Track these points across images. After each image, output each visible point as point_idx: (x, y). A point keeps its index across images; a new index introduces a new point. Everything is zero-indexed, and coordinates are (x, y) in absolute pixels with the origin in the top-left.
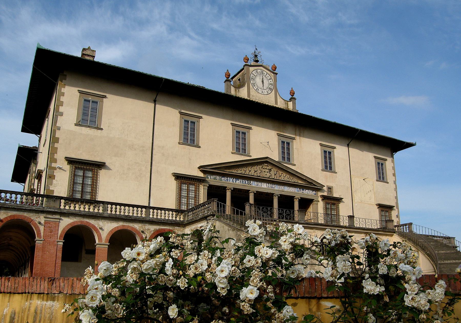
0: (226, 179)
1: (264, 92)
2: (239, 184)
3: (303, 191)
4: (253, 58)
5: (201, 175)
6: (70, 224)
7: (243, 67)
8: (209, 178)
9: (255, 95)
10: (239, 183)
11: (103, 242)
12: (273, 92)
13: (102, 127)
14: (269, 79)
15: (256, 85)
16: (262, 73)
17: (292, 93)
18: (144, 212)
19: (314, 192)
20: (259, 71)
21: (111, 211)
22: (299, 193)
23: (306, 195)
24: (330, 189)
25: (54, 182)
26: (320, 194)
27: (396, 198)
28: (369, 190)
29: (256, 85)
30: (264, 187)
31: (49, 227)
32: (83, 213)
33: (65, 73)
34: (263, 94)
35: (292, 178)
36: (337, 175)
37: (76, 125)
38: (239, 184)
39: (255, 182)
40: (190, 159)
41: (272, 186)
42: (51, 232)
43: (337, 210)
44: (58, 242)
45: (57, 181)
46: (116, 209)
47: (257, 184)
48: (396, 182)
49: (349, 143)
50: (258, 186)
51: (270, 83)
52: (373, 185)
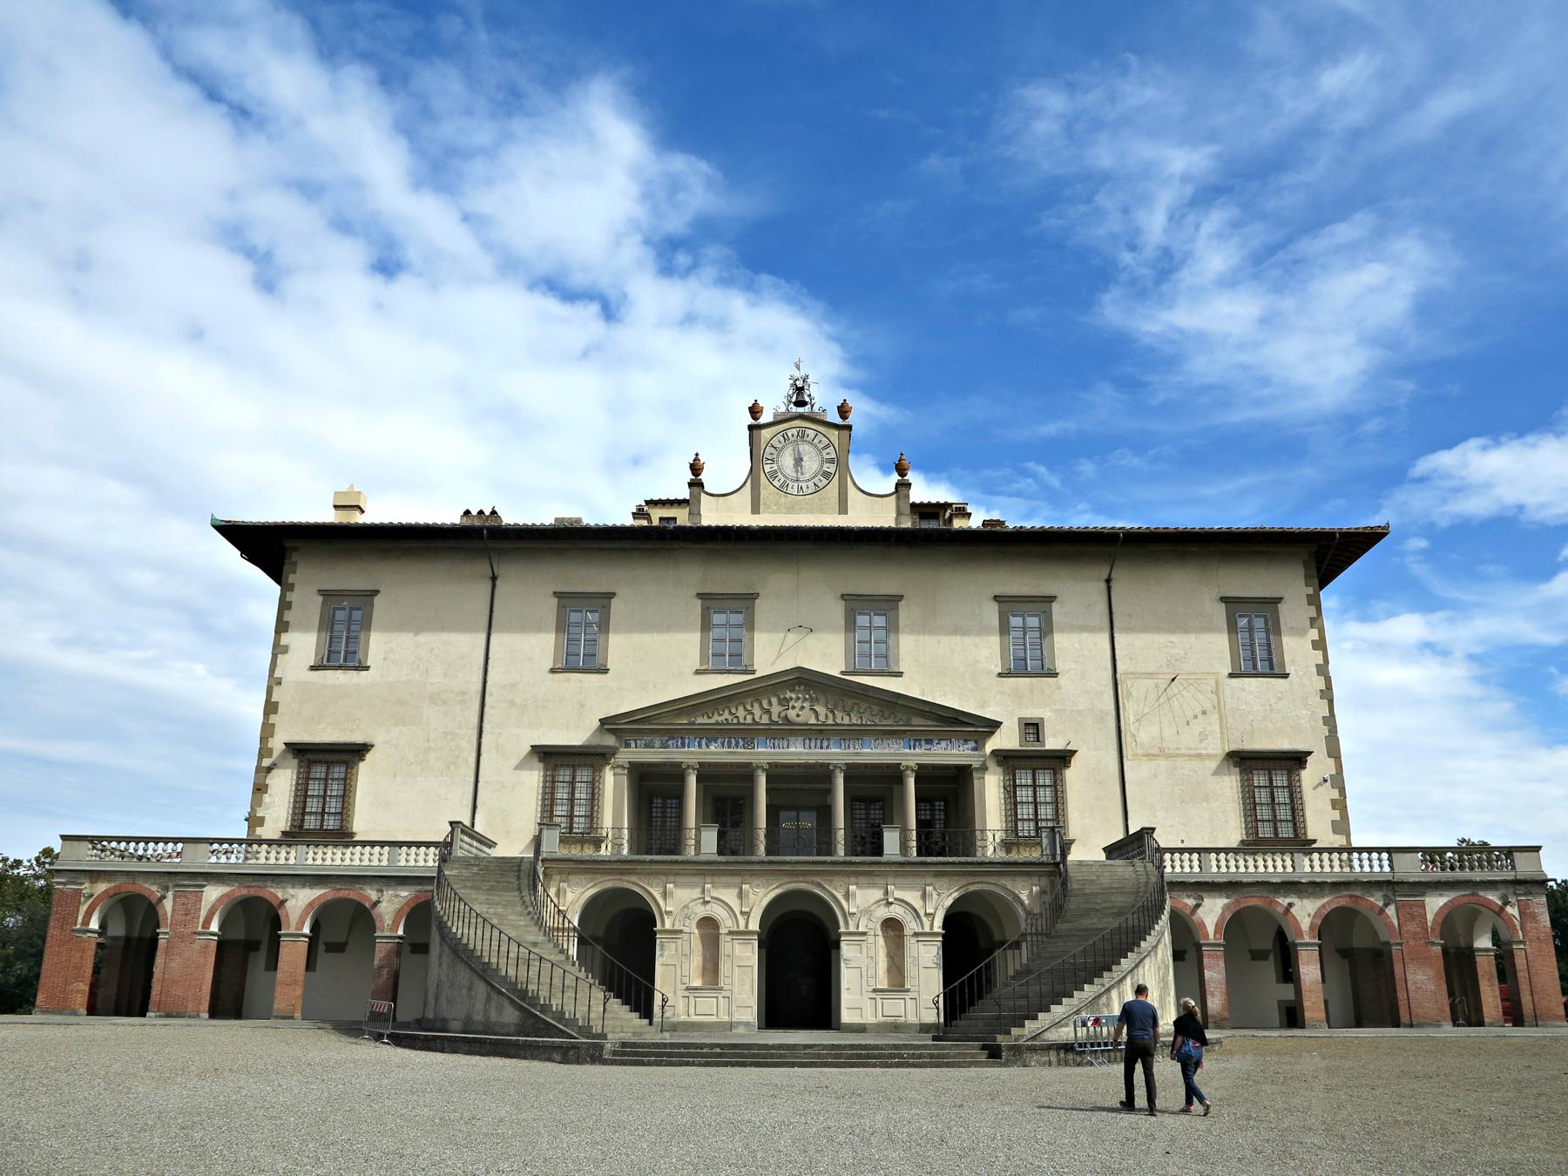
0: (679, 744)
2: (717, 752)
3: (928, 746)
5: (610, 741)
8: (633, 745)
13: (368, 665)
14: (827, 447)
18: (385, 857)
19: (971, 744)
26: (992, 744)
27: (1330, 721)
28: (1198, 711)
30: (797, 752)
31: (183, 904)
33: (293, 559)
34: (801, 493)
37: (313, 668)
39: (768, 741)
40: (583, 706)
41: (822, 743)
42: (186, 915)
43: (1058, 788)
44: (200, 934)
47: (774, 744)
48: (1330, 667)
49: (1110, 574)
51: (828, 457)
52: (1217, 694)
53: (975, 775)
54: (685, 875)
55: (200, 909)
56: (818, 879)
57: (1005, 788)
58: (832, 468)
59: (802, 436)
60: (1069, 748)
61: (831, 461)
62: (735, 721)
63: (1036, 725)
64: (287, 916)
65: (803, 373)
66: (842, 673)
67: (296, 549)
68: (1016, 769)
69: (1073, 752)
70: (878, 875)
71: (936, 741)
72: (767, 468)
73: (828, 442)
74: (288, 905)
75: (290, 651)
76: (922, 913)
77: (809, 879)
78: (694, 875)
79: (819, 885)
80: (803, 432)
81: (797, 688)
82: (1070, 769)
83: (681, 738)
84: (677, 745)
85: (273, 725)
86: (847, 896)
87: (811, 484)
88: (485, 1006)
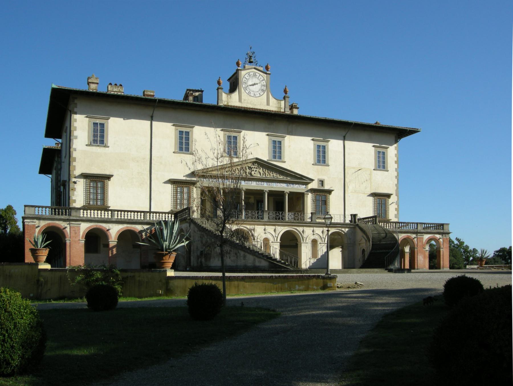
1: (256, 94)
6: (89, 228)
11: (113, 240)
12: (266, 93)
13: (109, 145)
14: (262, 81)
16: (255, 76)
19: (304, 186)
20: (251, 73)
21: (118, 216)
22: (287, 188)
23: (296, 189)
24: (322, 182)
25: (75, 193)
26: (311, 186)
30: (254, 185)
31: (74, 230)
32: (97, 219)
34: (255, 96)
36: (330, 167)
42: (75, 234)
45: (77, 192)
46: (121, 214)
50: (249, 185)
51: (263, 84)
55: (80, 232)
56: (295, 227)
57: (313, 200)
59: (255, 75)
61: (264, 85)
64: (111, 235)
65: (252, 50)
66: (267, 160)
67: (76, 98)
72: (244, 86)
73: (263, 79)
74: (110, 231)
75: (78, 138)
76: (322, 237)
80: (255, 74)
81: (255, 164)
82: (331, 195)
85: (75, 166)
87: (258, 93)
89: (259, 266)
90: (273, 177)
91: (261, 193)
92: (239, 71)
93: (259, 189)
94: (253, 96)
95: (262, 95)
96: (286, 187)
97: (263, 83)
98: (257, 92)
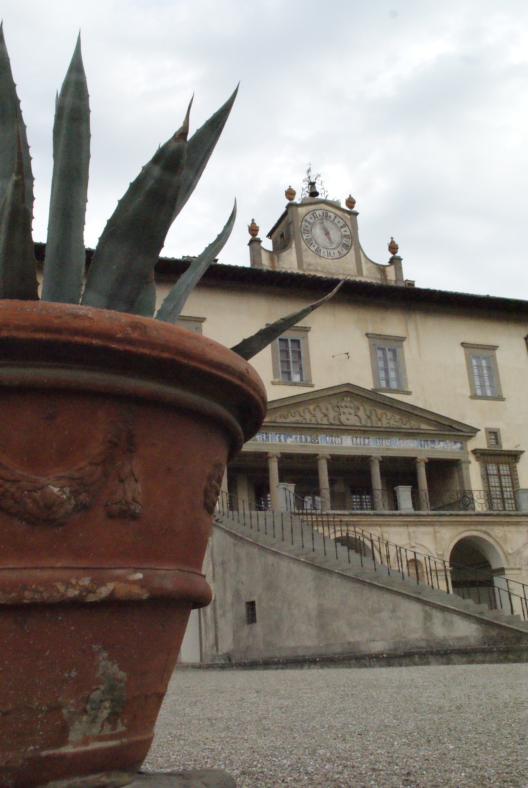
0: (264, 438)
1: (332, 254)
3: (433, 446)
4: (307, 189)
7: (284, 209)
9: (313, 261)
10: (292, 442)
12: (352, 251)
15: (313, 241)
16: (327, 216)
17: (393, 248)
19: (459, 445)
20: (318, 213)
23: (440, 452)
26: (472, 445)
29: (313, 241)
34: (330, 258)
35: (405, 420)
38: (293, 443)
39: (328, 438)
41: (364, 441)
43: (513, 475)
51: (346, 233)
53: (464, 466)
54: (395, 525)
56: (484, 528)
58: (349, 242)
60: (519, 449)
62: (304, 421)
63: (496, 433)
68: (488, 463)
69: (522, 452)
70: (521, 525)
71: (437, 442)
72: (305, 237)
77: (479, 528)
78: (400, 526)
79: (486, 533)
80: (327, 214)
81: (345, 399)
83: (266, 433)
84: (263, 439)
86: (505, 539)
87: (336, 252)
88: (425, 624)
89: (445, 639)
90: (388, 425)
91: (366, 460)
92: (294, 208)
93: (360, 454)
94: (327, 257)
95: (345, 255)
96: (420, 448)
97: (345, 231)
98: (334, 249)
